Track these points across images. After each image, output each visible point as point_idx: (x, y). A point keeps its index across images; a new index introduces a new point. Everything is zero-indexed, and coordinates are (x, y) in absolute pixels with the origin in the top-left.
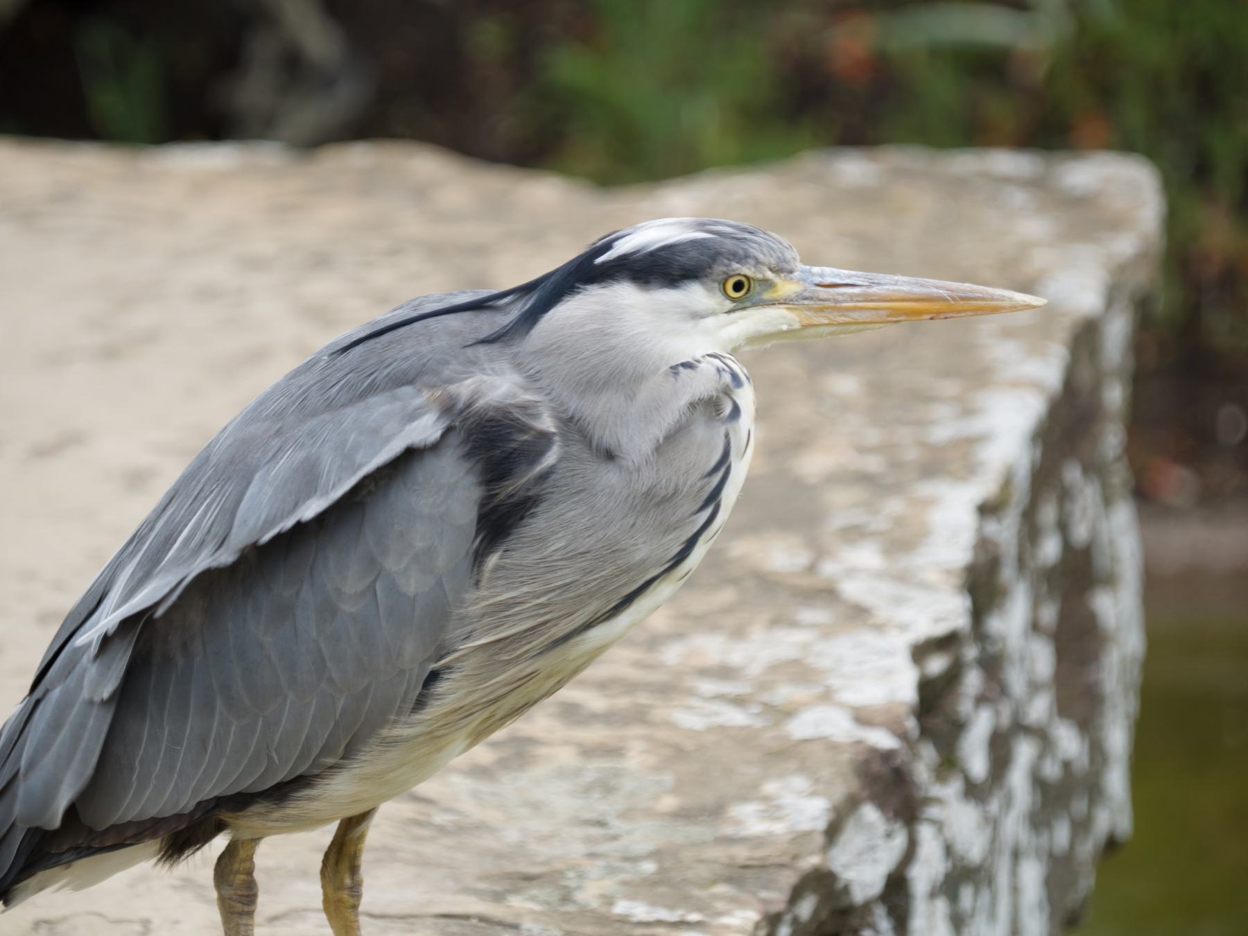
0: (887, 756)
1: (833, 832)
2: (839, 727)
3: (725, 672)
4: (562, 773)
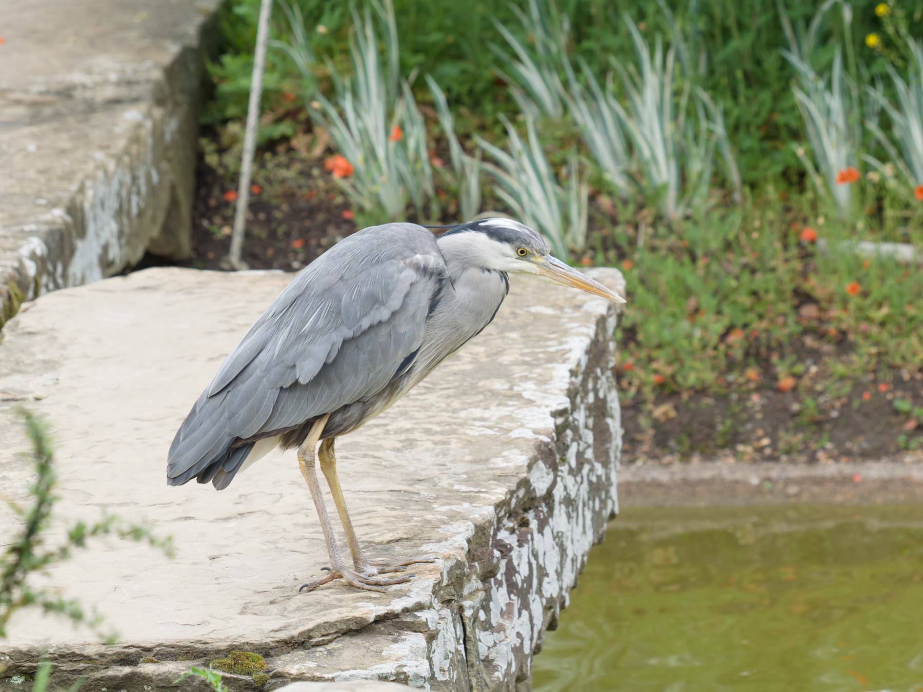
0: (547, 444)
1: (530, 467)
2: (530, 435)
3: (483, 419)
4: (427, 450)
